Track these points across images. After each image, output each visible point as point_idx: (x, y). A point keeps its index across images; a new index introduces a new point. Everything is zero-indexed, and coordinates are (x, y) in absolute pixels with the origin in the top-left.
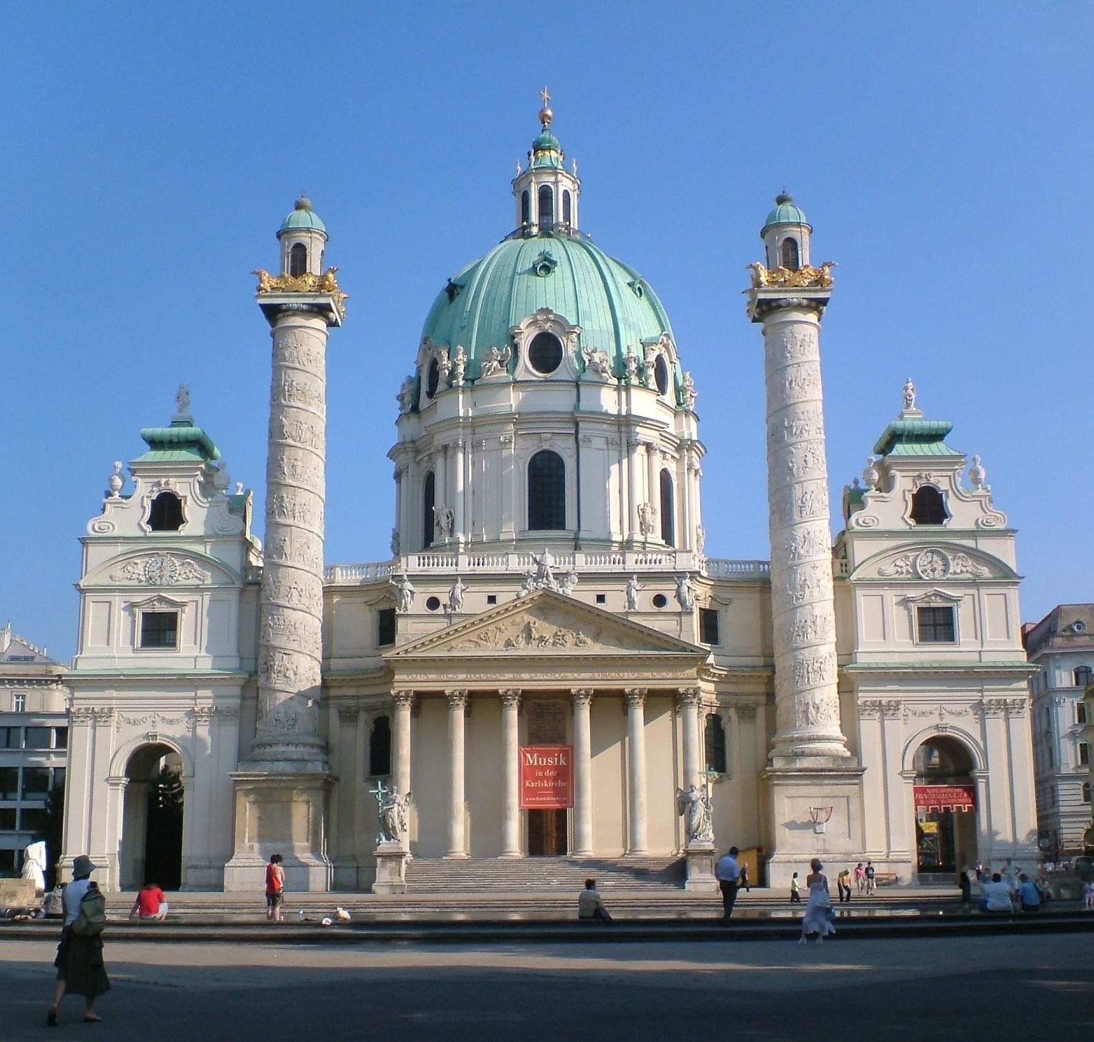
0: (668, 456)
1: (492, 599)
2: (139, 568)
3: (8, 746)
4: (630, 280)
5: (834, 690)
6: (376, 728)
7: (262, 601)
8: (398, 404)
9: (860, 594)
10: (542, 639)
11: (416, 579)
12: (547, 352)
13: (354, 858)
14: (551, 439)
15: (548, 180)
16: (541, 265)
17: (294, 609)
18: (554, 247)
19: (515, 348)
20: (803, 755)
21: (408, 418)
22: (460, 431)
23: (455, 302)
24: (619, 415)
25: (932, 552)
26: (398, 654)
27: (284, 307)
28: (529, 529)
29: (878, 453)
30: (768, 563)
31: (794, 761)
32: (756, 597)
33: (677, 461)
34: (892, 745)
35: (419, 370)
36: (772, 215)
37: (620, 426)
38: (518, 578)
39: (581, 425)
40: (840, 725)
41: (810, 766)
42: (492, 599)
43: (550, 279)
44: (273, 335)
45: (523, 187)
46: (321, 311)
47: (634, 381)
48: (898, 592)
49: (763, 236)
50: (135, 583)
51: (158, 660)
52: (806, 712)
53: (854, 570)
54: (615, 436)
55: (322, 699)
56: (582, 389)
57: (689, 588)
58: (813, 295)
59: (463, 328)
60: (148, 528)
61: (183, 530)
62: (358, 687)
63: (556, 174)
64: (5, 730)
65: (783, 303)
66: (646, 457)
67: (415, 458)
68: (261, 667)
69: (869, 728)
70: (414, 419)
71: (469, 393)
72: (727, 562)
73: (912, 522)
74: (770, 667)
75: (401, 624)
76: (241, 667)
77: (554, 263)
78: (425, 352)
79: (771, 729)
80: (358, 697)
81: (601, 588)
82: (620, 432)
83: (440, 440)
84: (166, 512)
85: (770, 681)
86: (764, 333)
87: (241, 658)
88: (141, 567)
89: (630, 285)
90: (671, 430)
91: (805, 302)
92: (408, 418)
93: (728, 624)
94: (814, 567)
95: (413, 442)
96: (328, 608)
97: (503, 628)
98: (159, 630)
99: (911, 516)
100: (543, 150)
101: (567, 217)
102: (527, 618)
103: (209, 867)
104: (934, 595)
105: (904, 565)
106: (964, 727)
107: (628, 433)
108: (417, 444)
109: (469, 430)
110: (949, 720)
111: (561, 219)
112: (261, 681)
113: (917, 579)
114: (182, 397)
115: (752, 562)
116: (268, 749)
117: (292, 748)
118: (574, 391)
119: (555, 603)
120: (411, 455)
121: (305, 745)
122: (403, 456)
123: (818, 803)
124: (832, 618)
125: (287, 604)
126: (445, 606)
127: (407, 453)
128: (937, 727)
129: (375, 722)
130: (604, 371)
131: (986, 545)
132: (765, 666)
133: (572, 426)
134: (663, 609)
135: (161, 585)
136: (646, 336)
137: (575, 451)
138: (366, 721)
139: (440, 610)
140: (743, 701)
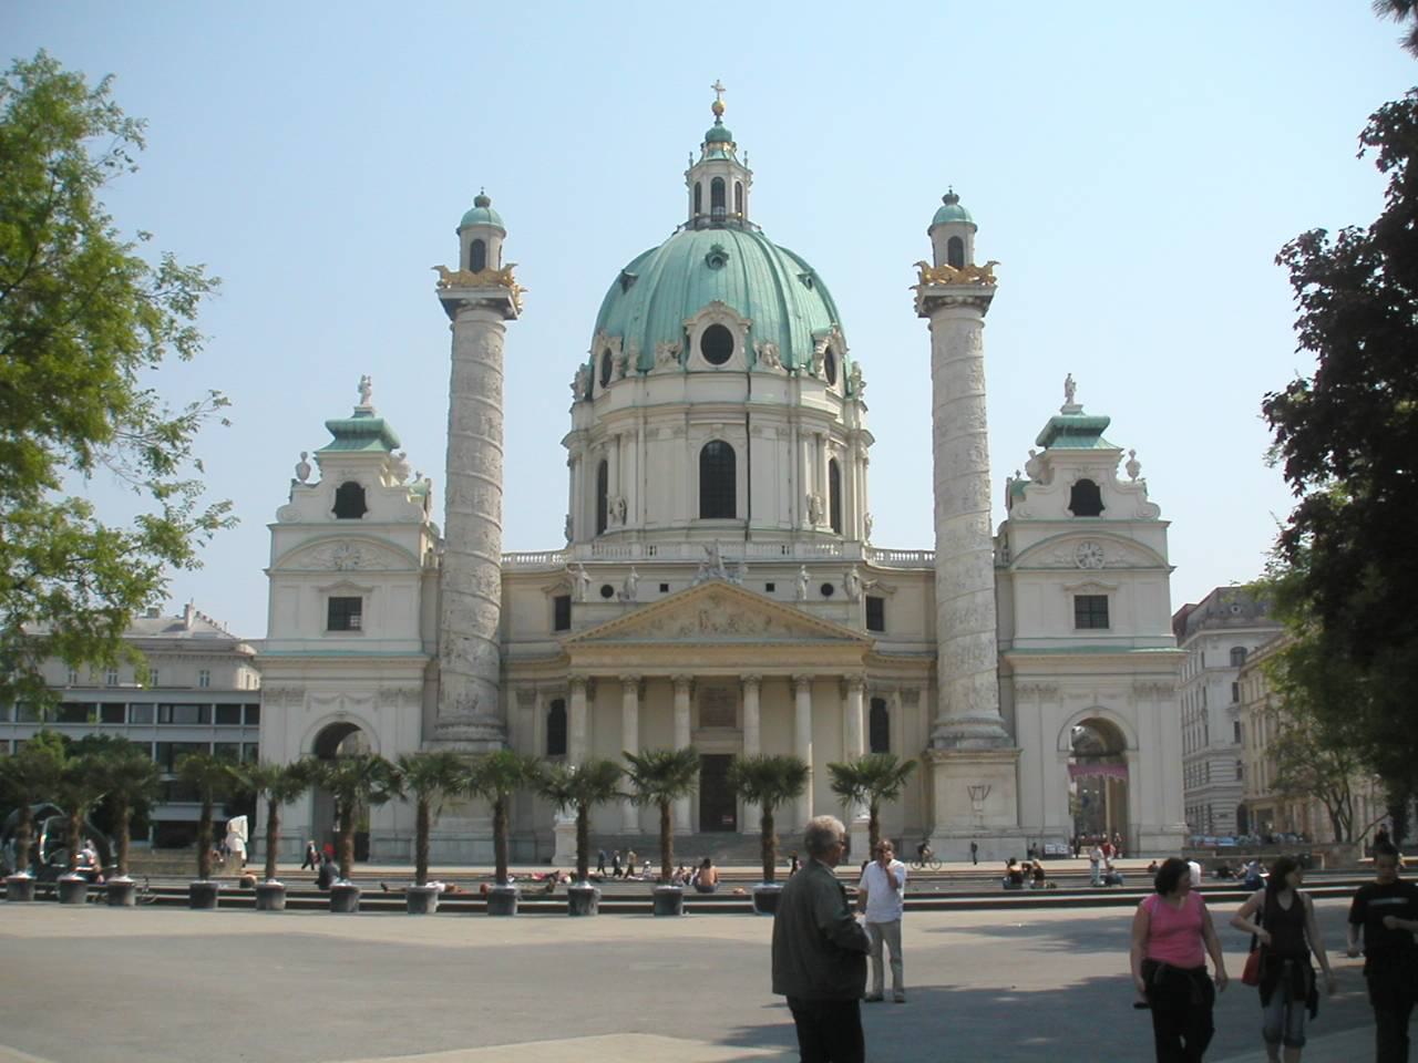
0: (837, 445)
1: (664, 588)
2: (326, 556)
3: (200, 721)
4: (800, 271)
5: (993, 677)
6: (553, 710)
7: (444, 587)
8: (572, 392)
11: (589, 568)
12: (718, 345)
13: (533, 832)
14: (723, 429)
15: (718, 171)
16: (713, 257)
18: (723, 238)
19: (688, 340)
20: (962, 737)
21: (582, 406)
22: (631, 421)
23: (628, 293)
24: (788, 406)
27: (464, 302)
28: (701, 518)
29: (1039, 445)
30: (932, 553)
31: (954, 743)
32: (921, 585)
33: (845, 450)
34: (1049, 729)
35: (593, 359)
36: (940, 213)
37: (789, 417)
38: (690, 567)
39: (752, 415)
40: (999, 709)
42: (664, 588)
43: (722, 274)
44: (452, 328)
45: (695, 179)
47: (804, 373)
49: (930, 232)
50: (323, 568)
51: (343, 642)
52: (966, 695)
53: (1018, 557)
54: (784, 426)
55: (501, 681)
56: (752, 380)
57: (856, 579)
58: (978, 293)
59: (636, 319)
60: (334, 516)
63: (728, 166)
64: (196, 709)
65: (948, 300)
66: (815, 447)
67: (588, 446)
68: (443, 650)
69: (1026, 711)
70: (587, 407)
71: (641, 385)
72: (893, 551)
73: (1071, 513)
74: (934, 655)
75: (576, 613)
76: (423, 650)
77: (727, 256)
78: (599, 341)
79: (934, 711)
80: (535, 681)
81: (771, 577)
82: (789, 422)
83: (614, 429)
84: (350, 501)
85: (933, 666)
86: (930, 328)
87: (423, 643)
89: (800, 276)
90: (840, 421)
91: (970, 300)
92: (582, 406)
93: (894, 614)
94: (978, 558)
95: (587, 430)
96: (505, 598)
98: (343, 613)
100: (714, 142)
101: (739, 207)
103: (396, 840)
104: (1091, 584)
107: (797, 423)
108: (591, 432)
109: (641, 421)
110: (1103, 702)
111: (733, 211)
112: (443, 664)
114: (363, 388)
115: (917, 552)
116: (450, 729)
117: (473, 729)
118: (746, 381)
120: (584, 443)
121: (485, 725)
122: (575, 445)
123: (977, 782)
124: (993, 606)
125: (466, 591)
126: (619, 595)
127: (580, 441)
128: (1089, 709)
130: (774, 363)
131: (1140, 535)
132: (928, 652)
133: (744, 416)
134: (832, 598)
135: (346, 570)
136: (815, 328)
137: (746, 441)
139: (614, 598)
140: (907, 685)
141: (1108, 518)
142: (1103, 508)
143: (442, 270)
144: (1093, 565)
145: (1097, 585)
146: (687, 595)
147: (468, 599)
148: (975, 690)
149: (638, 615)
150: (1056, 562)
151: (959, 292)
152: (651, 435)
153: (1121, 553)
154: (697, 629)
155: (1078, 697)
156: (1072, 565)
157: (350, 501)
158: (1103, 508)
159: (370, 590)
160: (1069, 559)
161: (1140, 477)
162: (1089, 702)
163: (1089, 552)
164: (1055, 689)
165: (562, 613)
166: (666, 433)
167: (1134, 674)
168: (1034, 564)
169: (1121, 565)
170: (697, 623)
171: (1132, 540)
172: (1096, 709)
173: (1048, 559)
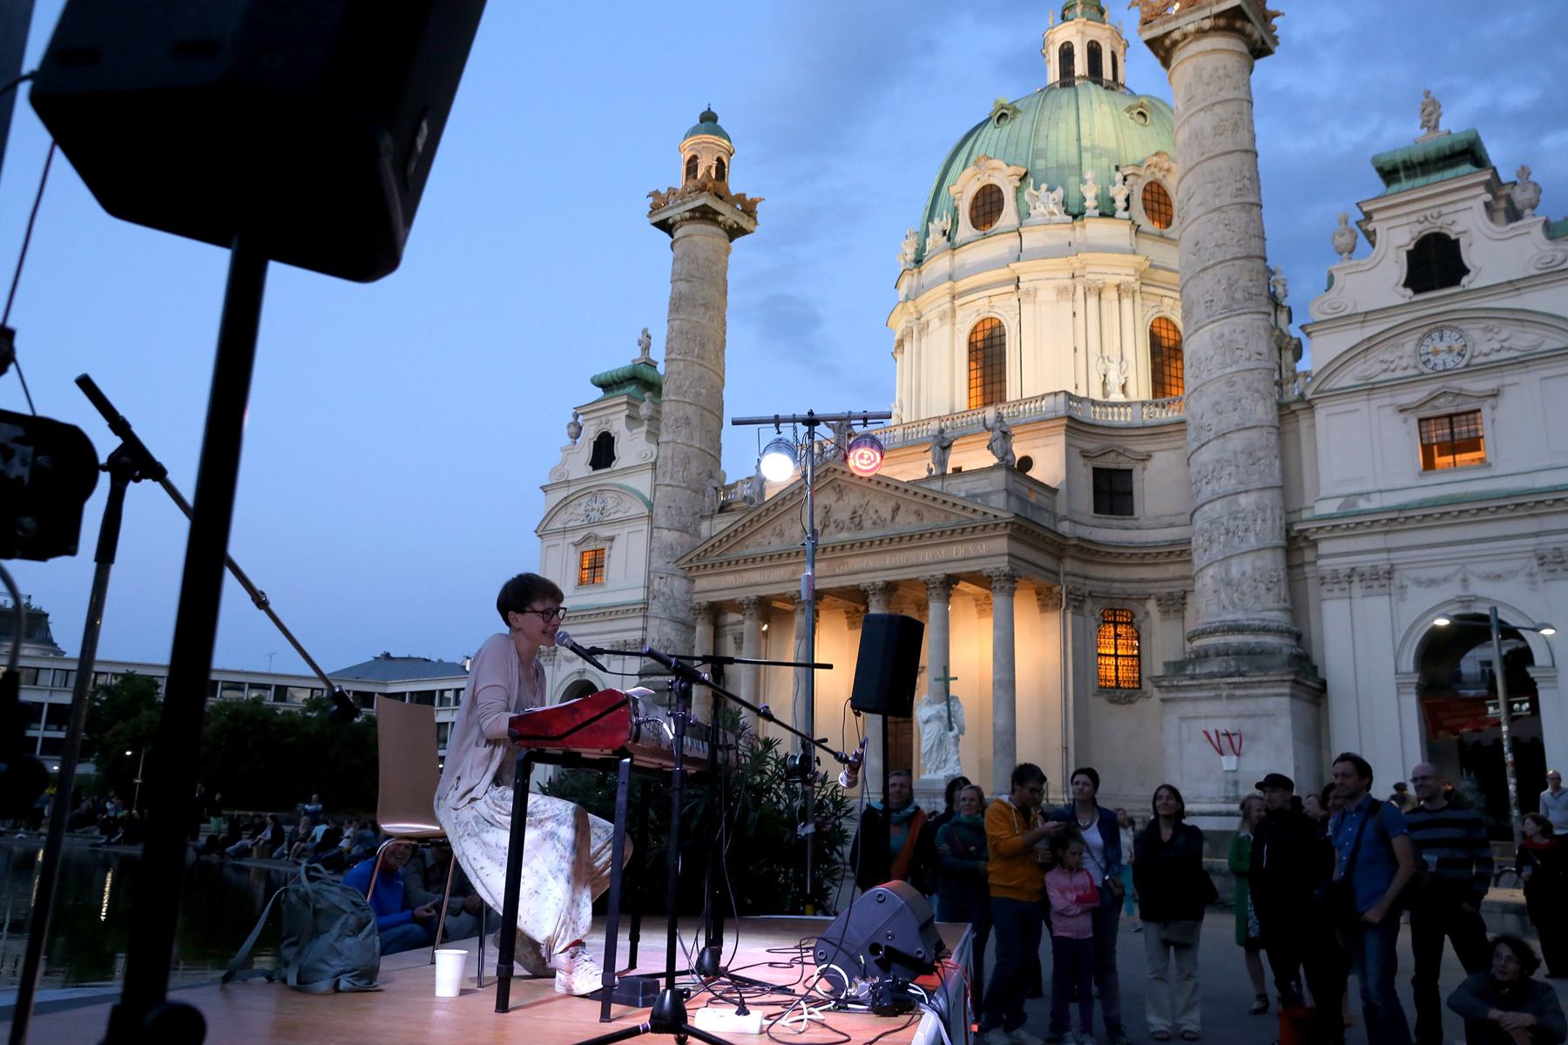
5: (1272, 562)
9: (1321, 413)
41: (1216, 669)
46: (705, 215)
48: (1387, 401)
61: (617, 465)
65: (1176, 35)
73: (1409, 292)
84: (603, 452)
88: (581, 510)
91: (1207, 24)
99: (1406, 285)
106: (1513, 598)
110: (1479, 588)
113: (1420, 379)
123: (1226, 725)
140: (1164, 591)
141: (1474, 286)
142: (1466, 271)
143: (656, 194)
144: (1450, 365)
147: (665, 533)
148: (1229, 583)
150: (1385, 371)
151: (1189, 19)
152: (924, 328)
153: (1503, 335)
155: (1432, 582)
157: (603, 452)
158: (1466, 271)
159: (612, 539)
160: (1404, 363)
162: (1453, 590)
163: (1442, 346)
164: (1390, 574)
166: (934, 324)
167: (1537, 534)
168: (1345, 380)
169: (1504, 355)
172: (1466, 601)
173: (1369, 367)
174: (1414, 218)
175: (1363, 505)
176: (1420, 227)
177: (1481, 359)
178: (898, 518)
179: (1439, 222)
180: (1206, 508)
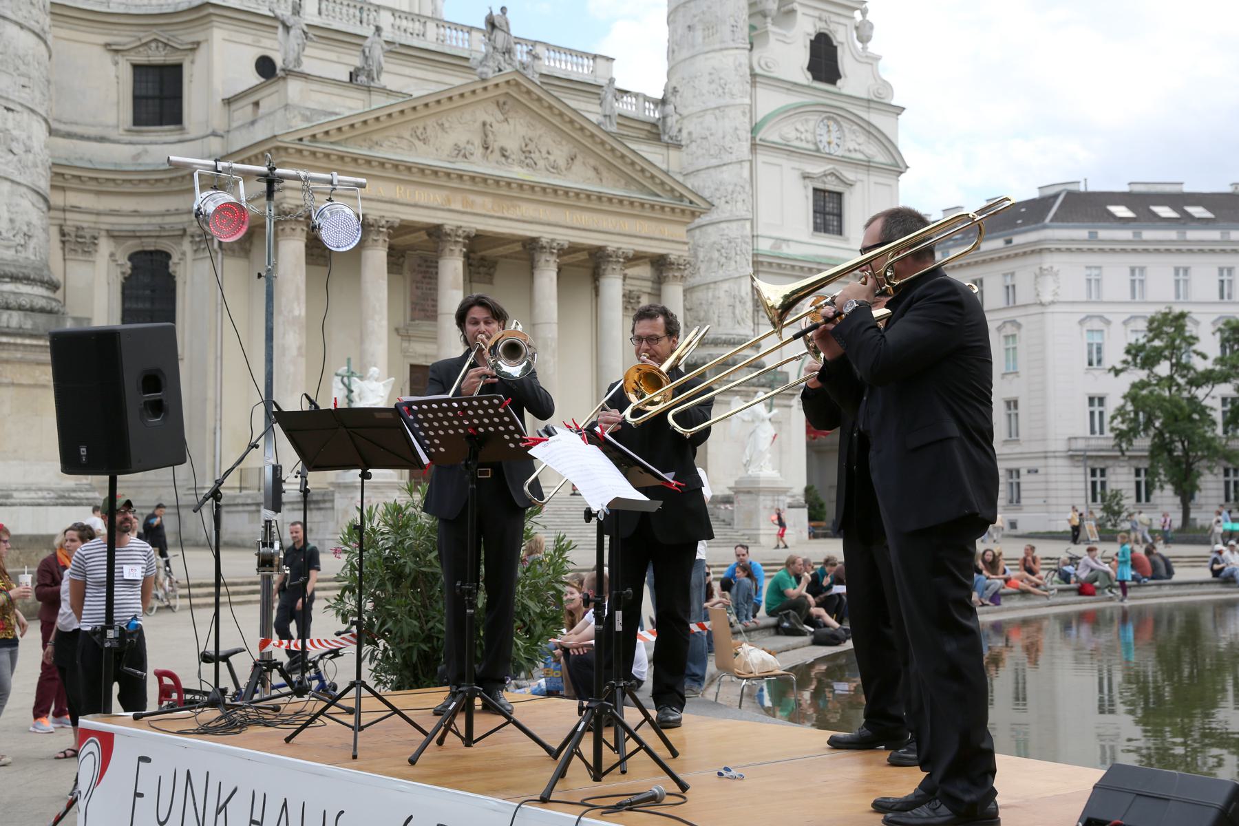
6: (134, 268)
10: (503, 153)
17: (22, 27)
25: (829, 118)
26: (301, 140)
48: (797, 165)
62: (99, 193)
73: (809, 75)
97: (447, 125)
102: (482, 116)
104: (832, 174)
105: (802, 129)
113: (816, 154)
119: (524, 99)
129: (131, 258)
138: (112, 255)
141: (844, 91)
145: (837, 177)
146: (474, 92)
147: (12, 30)
149: (402, 112)
154: (479, 151)
156: (812, 147)
160: (810, 137)
161: (872, 47)
165: (159, 95)
170: (478, 142)
171: (869, 123)
174: (817, 13)
175: (787, 250)
176: (821, 27)
177: (848, 154)
178: (574, 168)
179: (832, 27)
180: (723, 225)
